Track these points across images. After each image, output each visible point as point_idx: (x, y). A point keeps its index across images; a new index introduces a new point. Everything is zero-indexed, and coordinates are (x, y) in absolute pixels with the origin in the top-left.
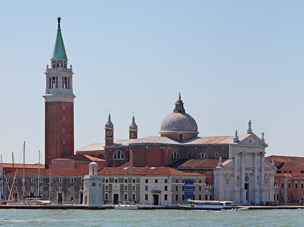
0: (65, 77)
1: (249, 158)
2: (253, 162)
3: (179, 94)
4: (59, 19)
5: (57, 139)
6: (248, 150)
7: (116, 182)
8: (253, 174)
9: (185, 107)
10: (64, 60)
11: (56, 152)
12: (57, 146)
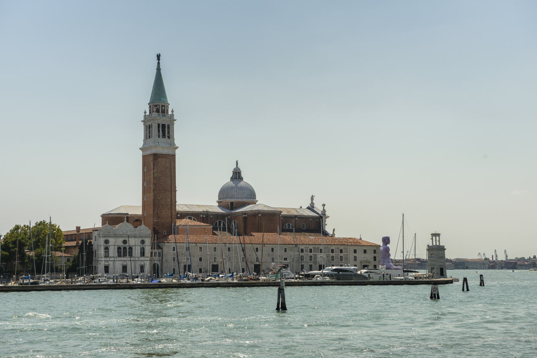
3: (237, 162)
5: (171, 199)
7: (321, 252)
11: (170, 215)
12: (171, 208)
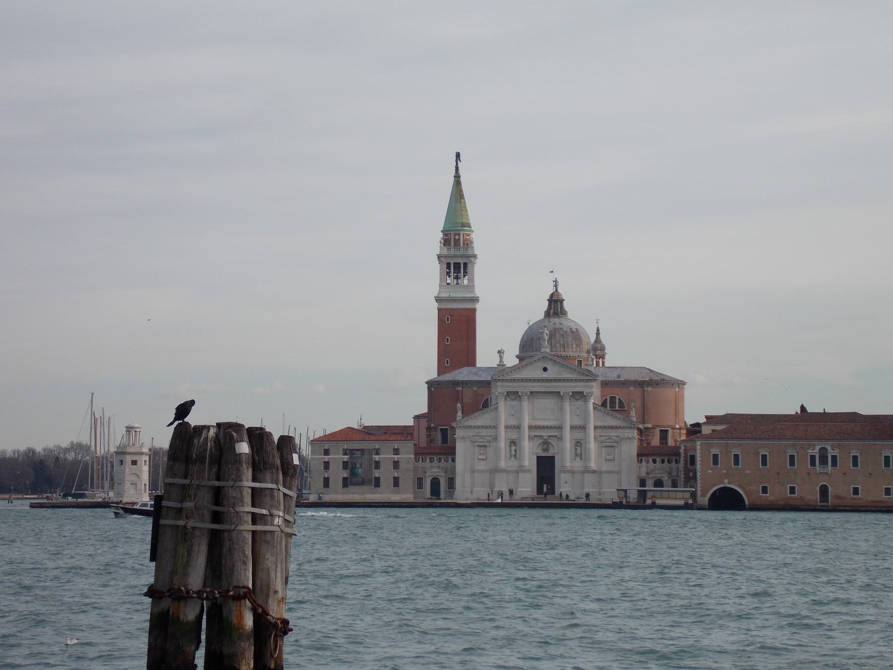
0: (454, 263)
1: (548, 403)
2: (561, 409)
3: (556, 281)
4: (458, 155)
6: (537, 387)
8: (560, 437)
9: (566, 305)
10: (452, 233)
